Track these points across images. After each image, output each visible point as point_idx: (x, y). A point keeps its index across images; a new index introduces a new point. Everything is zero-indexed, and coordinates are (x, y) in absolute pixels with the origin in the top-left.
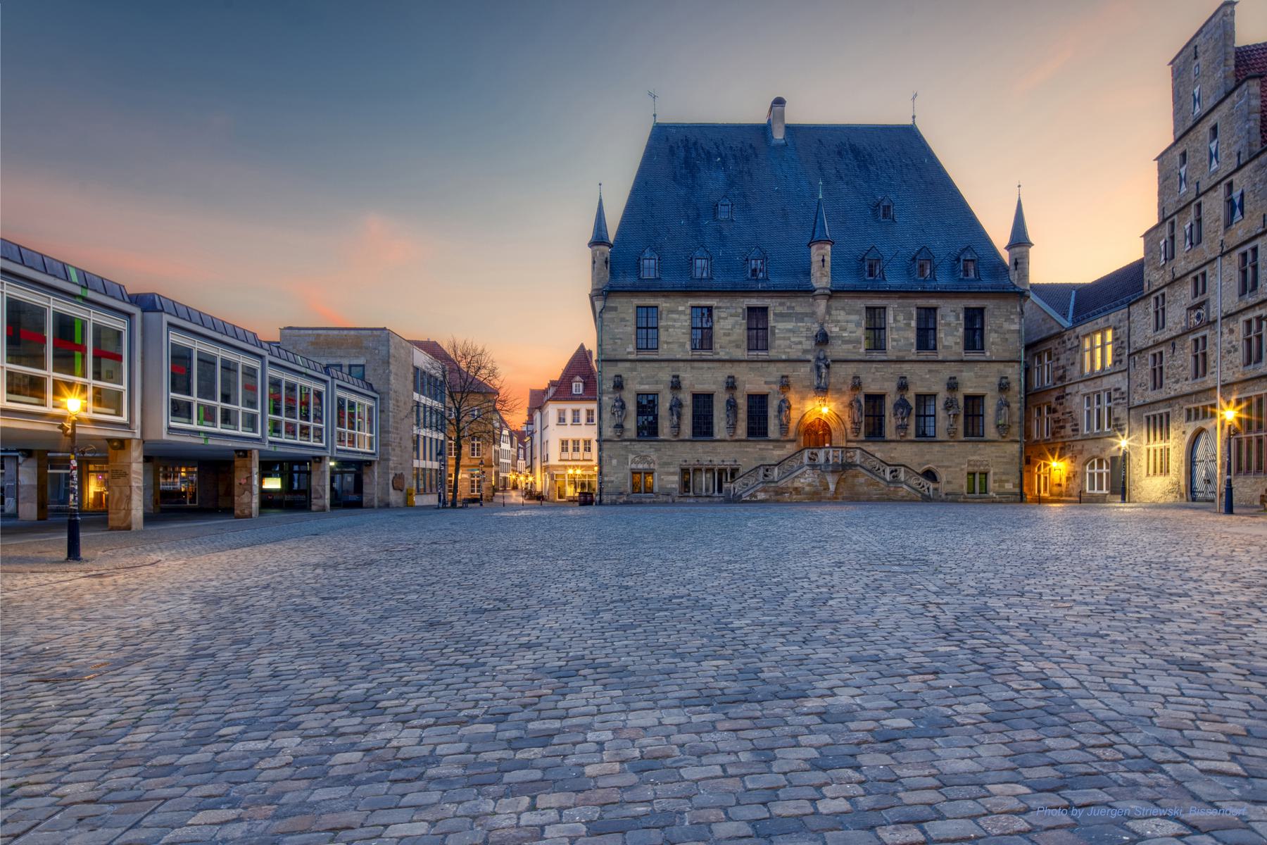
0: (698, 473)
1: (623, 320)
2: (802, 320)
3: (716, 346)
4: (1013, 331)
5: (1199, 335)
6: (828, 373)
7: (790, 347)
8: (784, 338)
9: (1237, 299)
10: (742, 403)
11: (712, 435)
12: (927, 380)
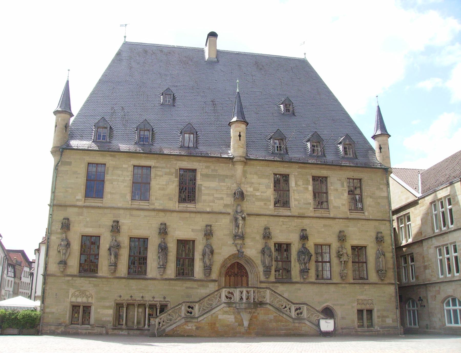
0: (131, 308)
2: (223, 181)
3: (153, 198)
4: (383, 198)
6: (244, 225)
7: (213, 202)
8: (209, 195)
10: (172, 247)
11: (145, 272)
12: (322, 233)
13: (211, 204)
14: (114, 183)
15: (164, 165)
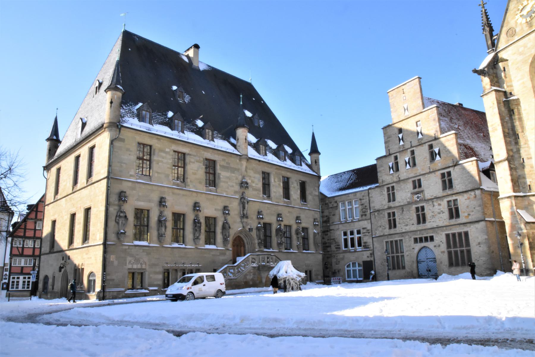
1: (128, 150)
2: (233, 172)
5: (420, 205)
9: (441, 191)
13: (226, 190)
14: (160, 164)
15: (194, 153)
